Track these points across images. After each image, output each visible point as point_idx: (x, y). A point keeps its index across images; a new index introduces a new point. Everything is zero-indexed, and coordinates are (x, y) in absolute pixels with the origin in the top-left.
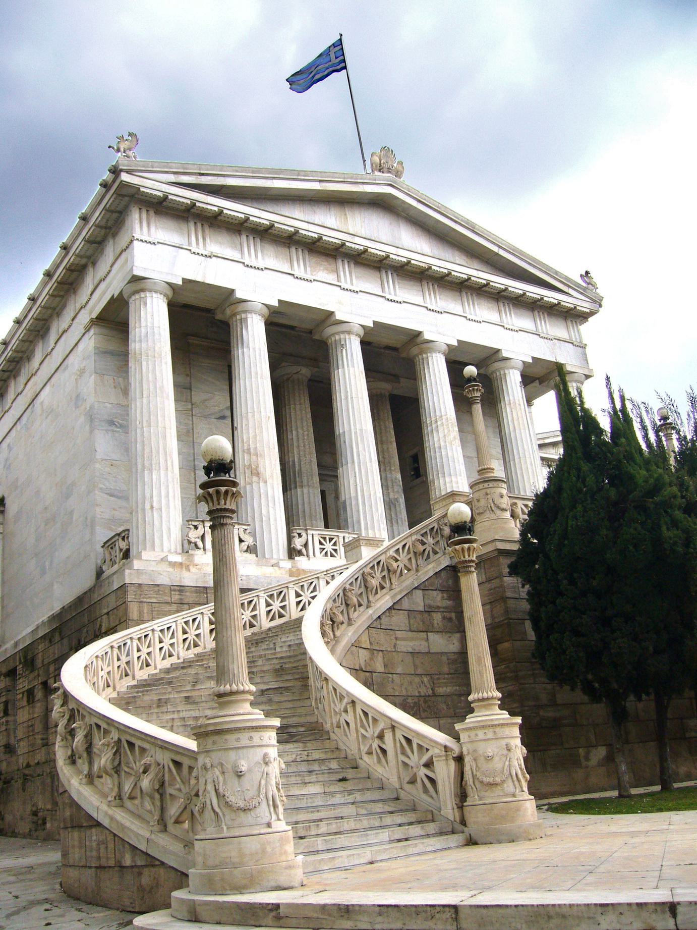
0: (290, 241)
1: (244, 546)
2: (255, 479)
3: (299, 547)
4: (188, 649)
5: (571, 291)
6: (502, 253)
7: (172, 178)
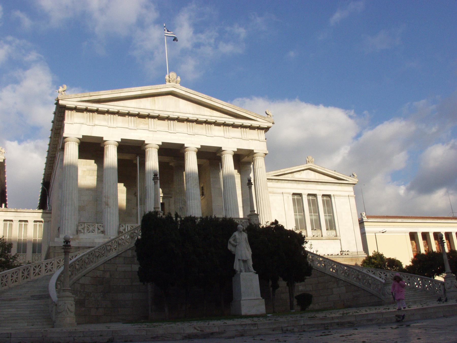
1: (100, 231)
2: (106, 207)
3: (121, 230)
4: (35, 275)
5: (258, 119)
7: (79, 99)
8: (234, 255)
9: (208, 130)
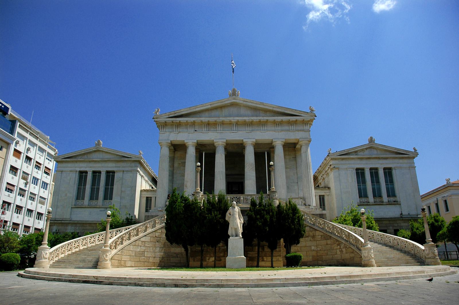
0: (202, 124)
5: (302, 115)
6: (275, 109)
7: (168, 117)
8: (229, 223)
9: (262, 127)
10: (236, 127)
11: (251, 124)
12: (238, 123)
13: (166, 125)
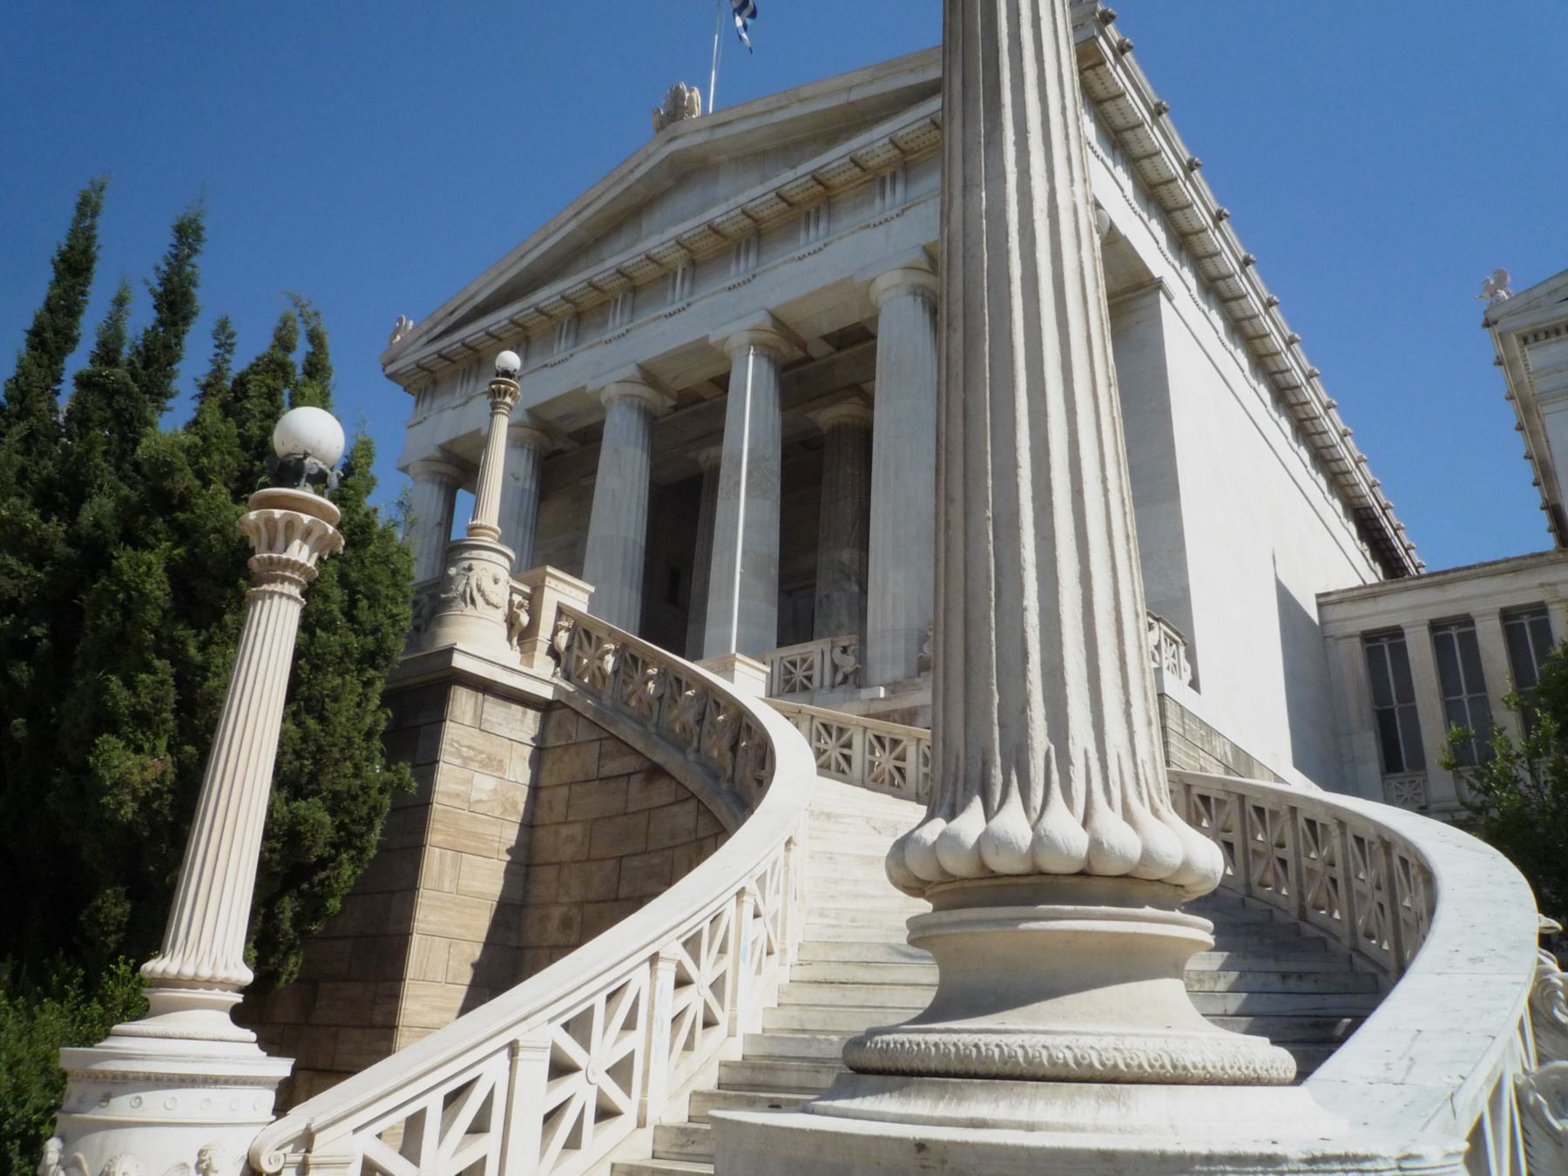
6: (855, 96)
7: (425, 339)
10: (687, 284)
11: (754, 236)
12: (698, 257)
13: (435, 383)
